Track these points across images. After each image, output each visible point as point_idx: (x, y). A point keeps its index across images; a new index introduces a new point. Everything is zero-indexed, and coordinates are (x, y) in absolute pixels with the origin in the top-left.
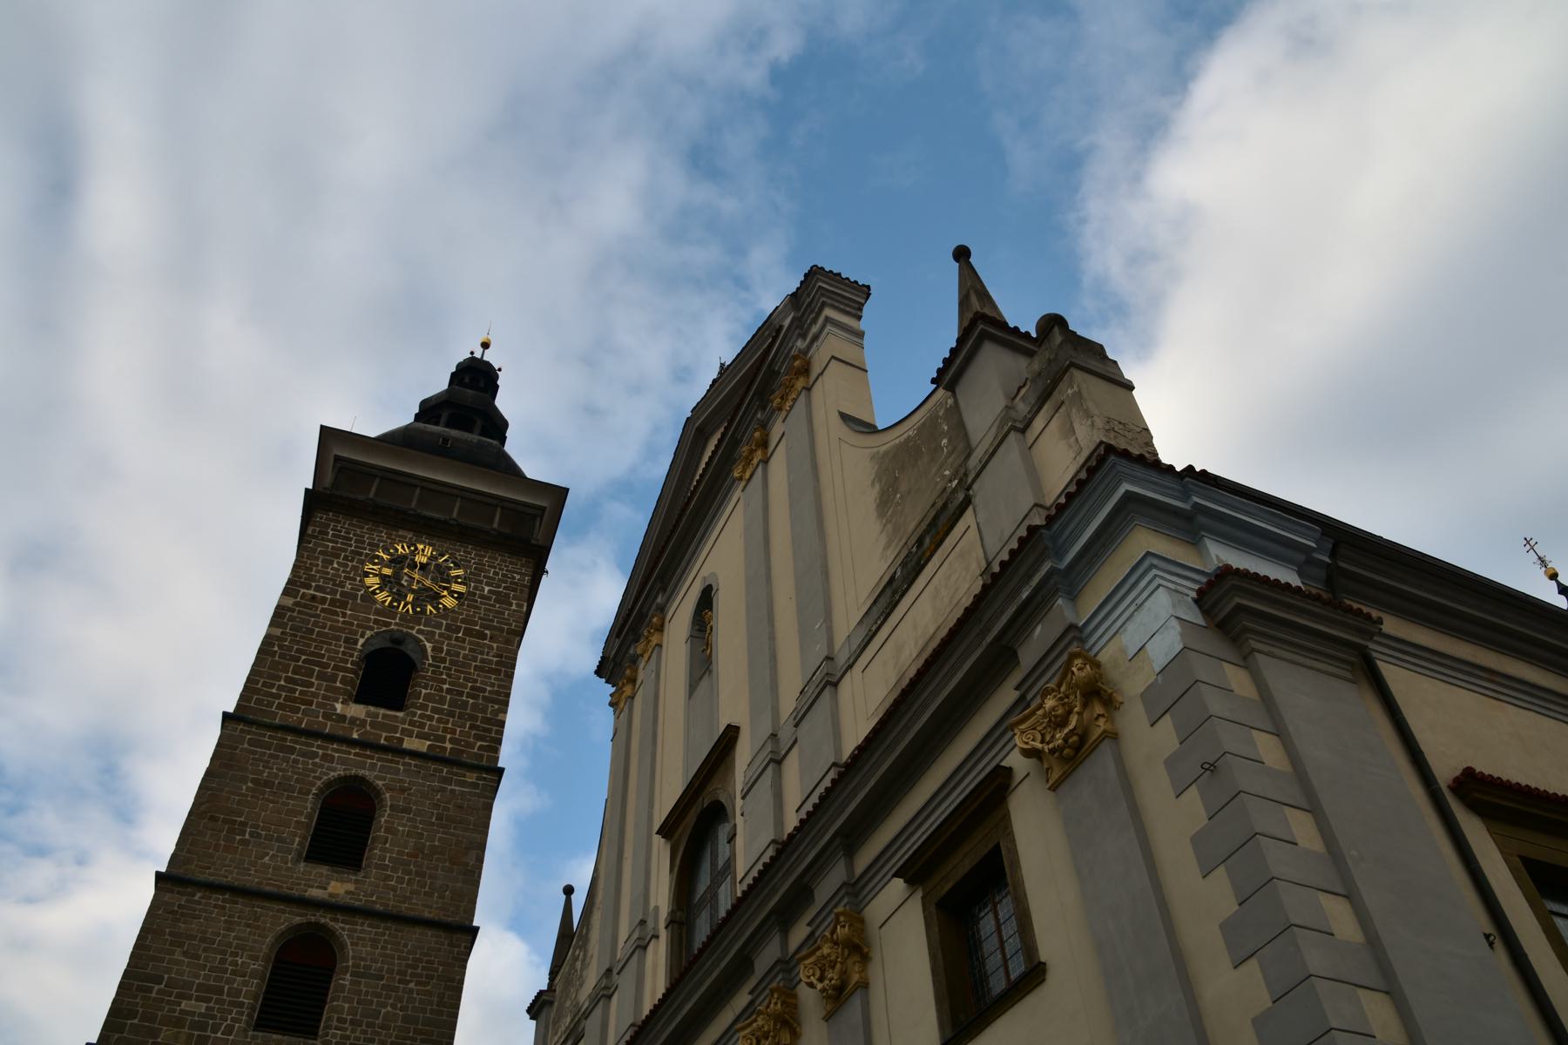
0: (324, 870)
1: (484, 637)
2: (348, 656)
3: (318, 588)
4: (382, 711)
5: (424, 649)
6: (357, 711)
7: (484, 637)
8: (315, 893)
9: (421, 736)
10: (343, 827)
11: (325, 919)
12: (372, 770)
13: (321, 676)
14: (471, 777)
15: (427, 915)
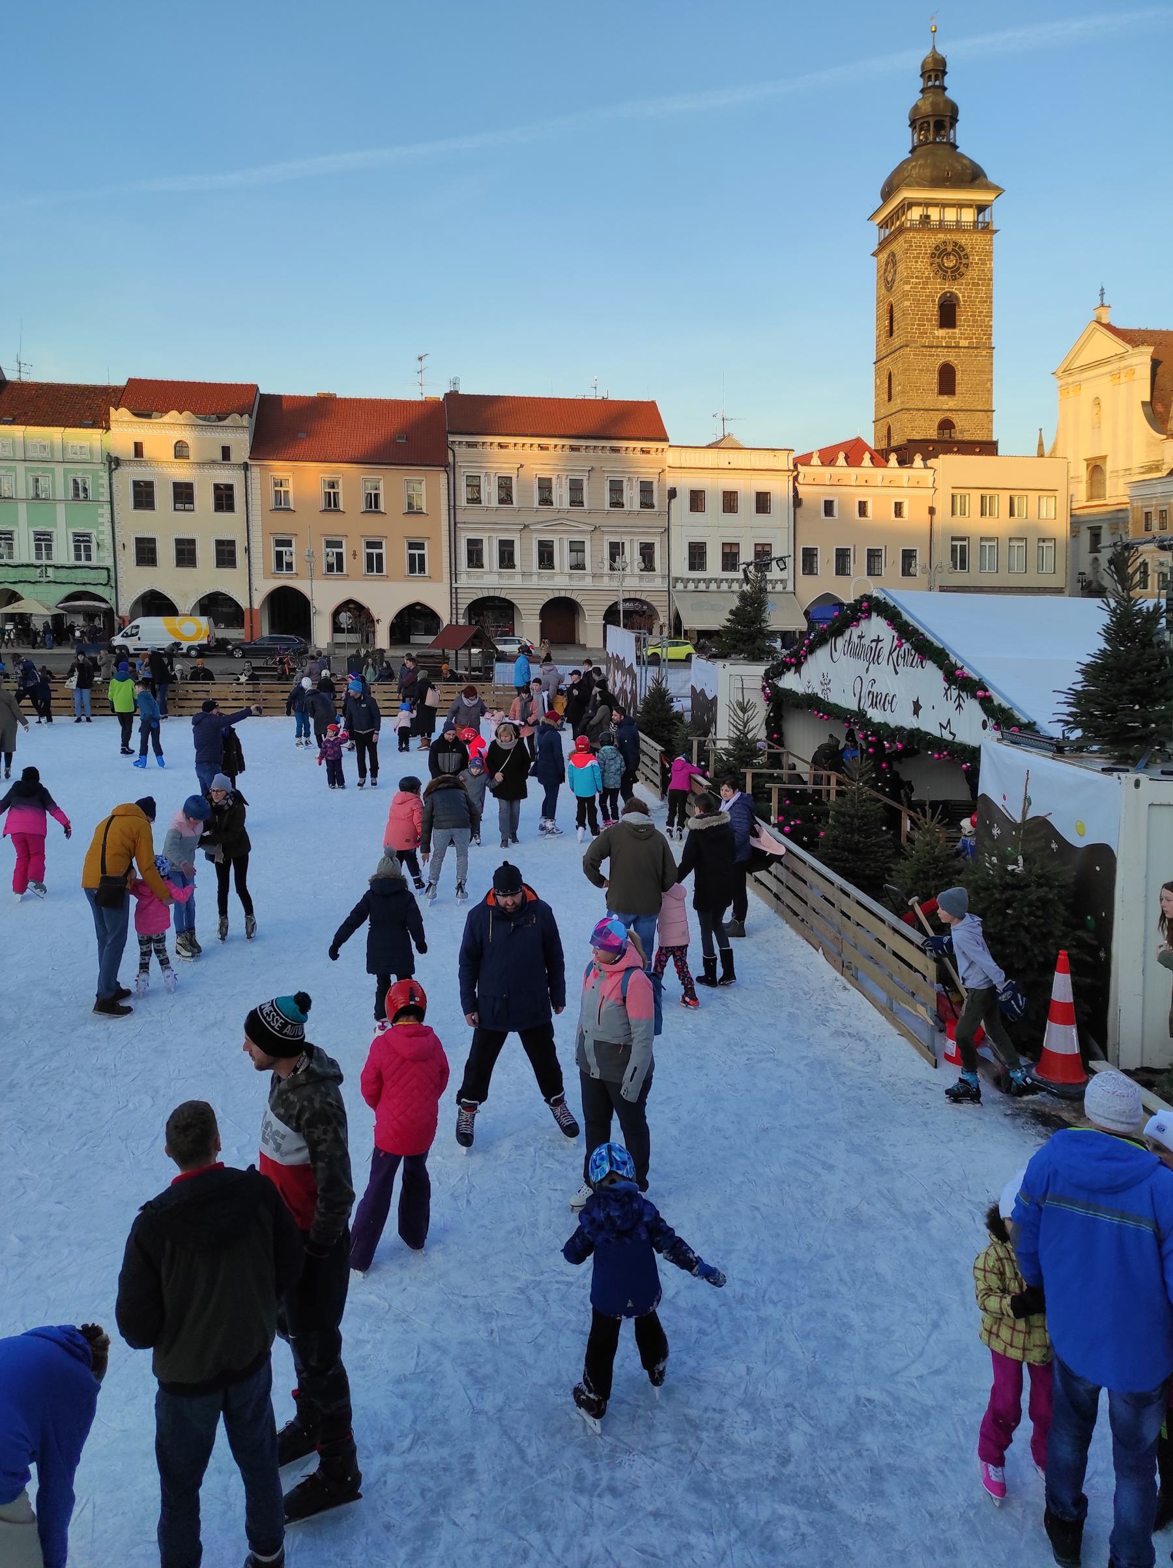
0: (946, 397)
1: (978, 285)
2: (933, 309)
3: (917, 277)
4: (951, 331)
5: (957, 298)
6: (942, 332)
7: (978, 285)
8: (945, 407)
9: (966, 339)
10: (947, 380)
11: (948, 415)
12: (951, 357)
13: (928, 320)
14: (984, 353)
15: (979, 408)
